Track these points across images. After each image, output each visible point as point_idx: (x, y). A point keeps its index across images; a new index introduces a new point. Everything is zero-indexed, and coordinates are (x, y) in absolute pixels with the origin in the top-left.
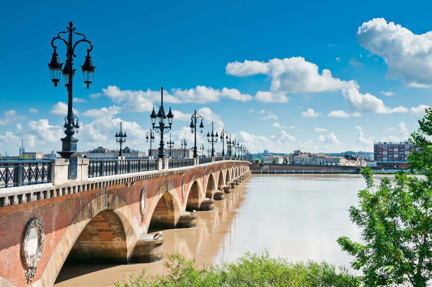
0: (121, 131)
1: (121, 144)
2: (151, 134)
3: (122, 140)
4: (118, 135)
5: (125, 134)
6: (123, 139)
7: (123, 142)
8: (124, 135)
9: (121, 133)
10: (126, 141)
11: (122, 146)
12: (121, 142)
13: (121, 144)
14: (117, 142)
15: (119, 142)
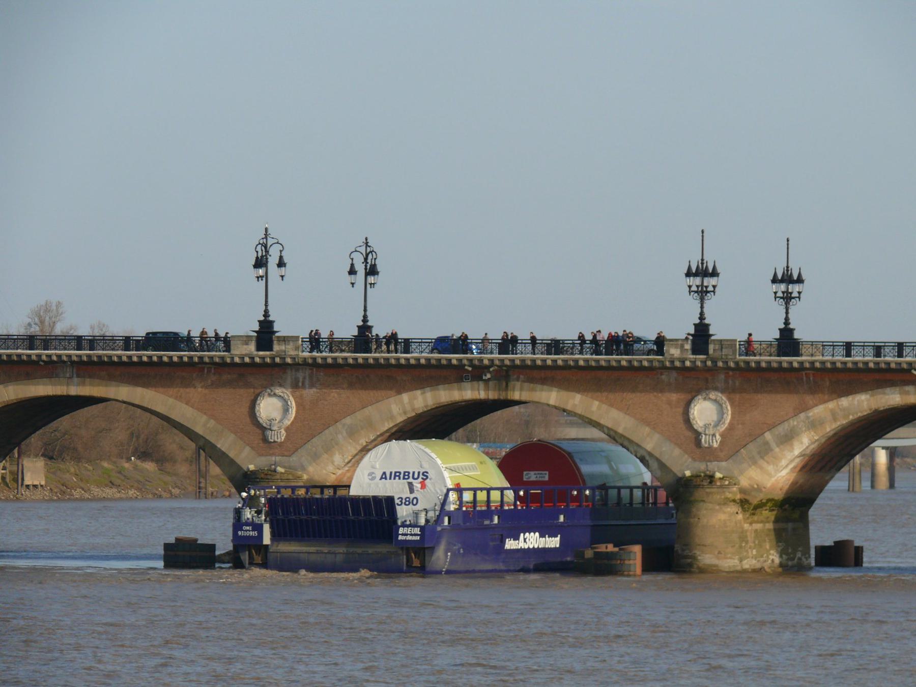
0: (788, 267)
1: (787, 304)
3: (791, 293)
4: (780, 276)
5: (800, 275)
6: (794, 289)
7: (794, 298)
8: (795, 277)
9: (788, 271)
10: (802, 295)
11: (790, 311)
12: (788, 298)
13: (787, 304)
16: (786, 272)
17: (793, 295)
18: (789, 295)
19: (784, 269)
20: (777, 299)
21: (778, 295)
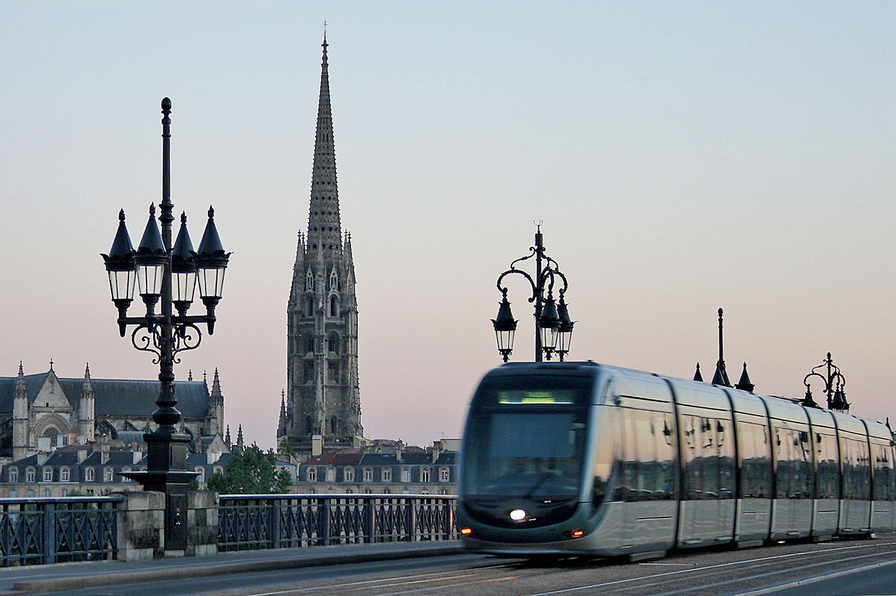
0: (166, 207)
2: (541, 279)
3: (183, 306)
4: (136, 242)
7: (191, 321)
8: (196, 243)
9: (167, 219)
10: (218, 310)
14: (123, 322)
16: (159, 224)
17: (189, 313)
18: (175, 312)
19: (152, 210)
21: (130, 313)
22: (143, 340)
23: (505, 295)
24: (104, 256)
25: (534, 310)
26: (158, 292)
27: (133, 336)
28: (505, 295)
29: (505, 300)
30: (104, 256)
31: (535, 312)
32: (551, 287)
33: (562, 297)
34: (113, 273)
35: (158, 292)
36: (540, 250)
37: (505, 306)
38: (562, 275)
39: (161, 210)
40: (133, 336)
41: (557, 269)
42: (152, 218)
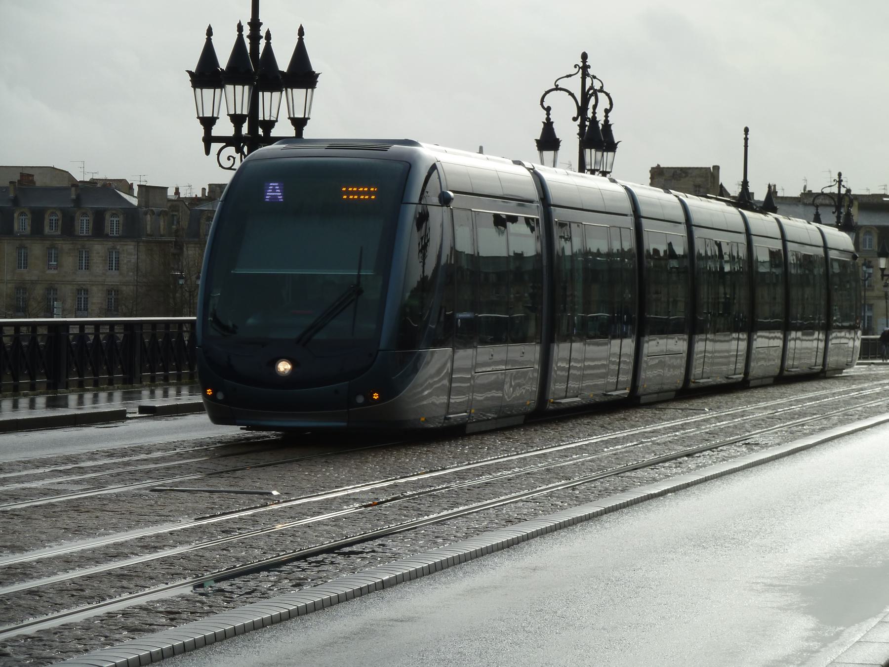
0: (255, 24)
3: (269, 125)
4: (223, 60)
5: (300, 54)
8: (283, 62)
9: (255, 37)
14: (208, 140)
15: (227, 141)
16: (247, 42)
17: (274, 133)
18: (261, 132)
19: (240, 28)
20: (215, 147)
21: (216, 131)
22: (229, 159)
23: (548, 114)
24: (190, 73)
25: (577, 130)
26: (245, 112)
27: (219, 154)
28: (548, 114)
29: (548, 119)
30: (190, 73)
31: (578, 131)
32: (595, 107)
33: (606, 116)
34: (198, 90)
35: (245, 112)
36: (585, 69)
37: (548, 126)
38: (608, 95)
39: (249, 28)
40: (219, 154)
41: (602, 87)
42: (240, 37)
